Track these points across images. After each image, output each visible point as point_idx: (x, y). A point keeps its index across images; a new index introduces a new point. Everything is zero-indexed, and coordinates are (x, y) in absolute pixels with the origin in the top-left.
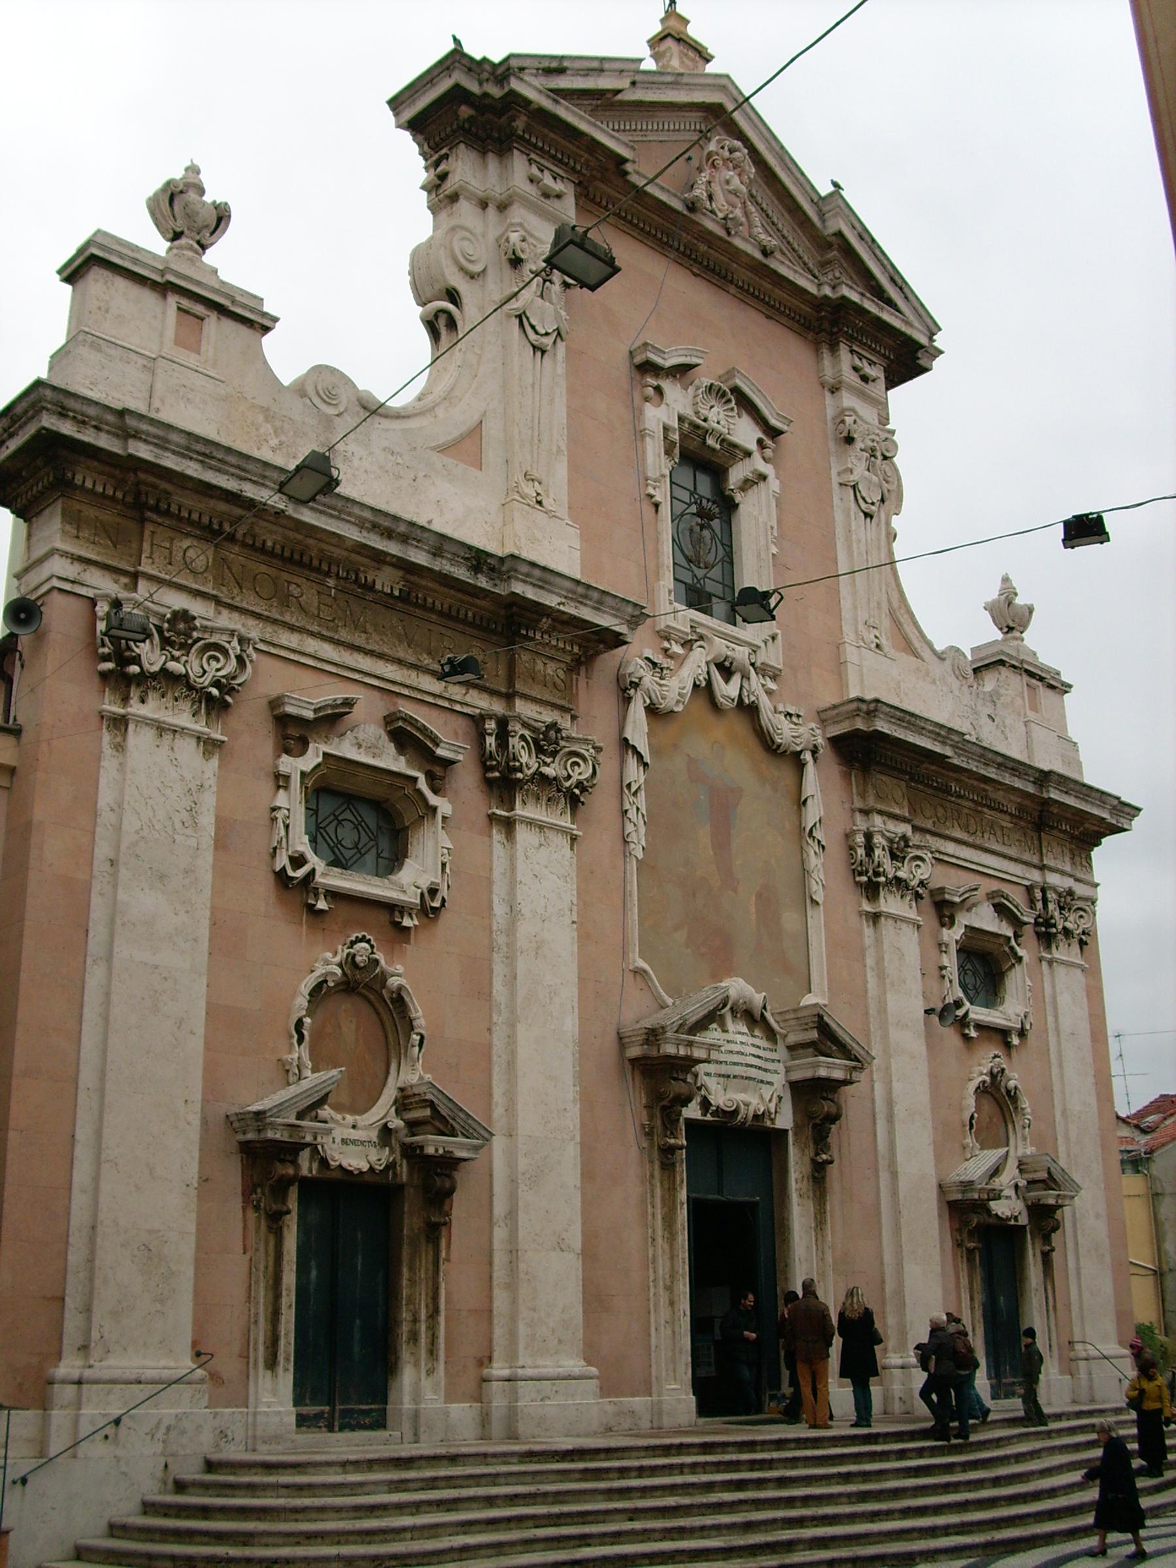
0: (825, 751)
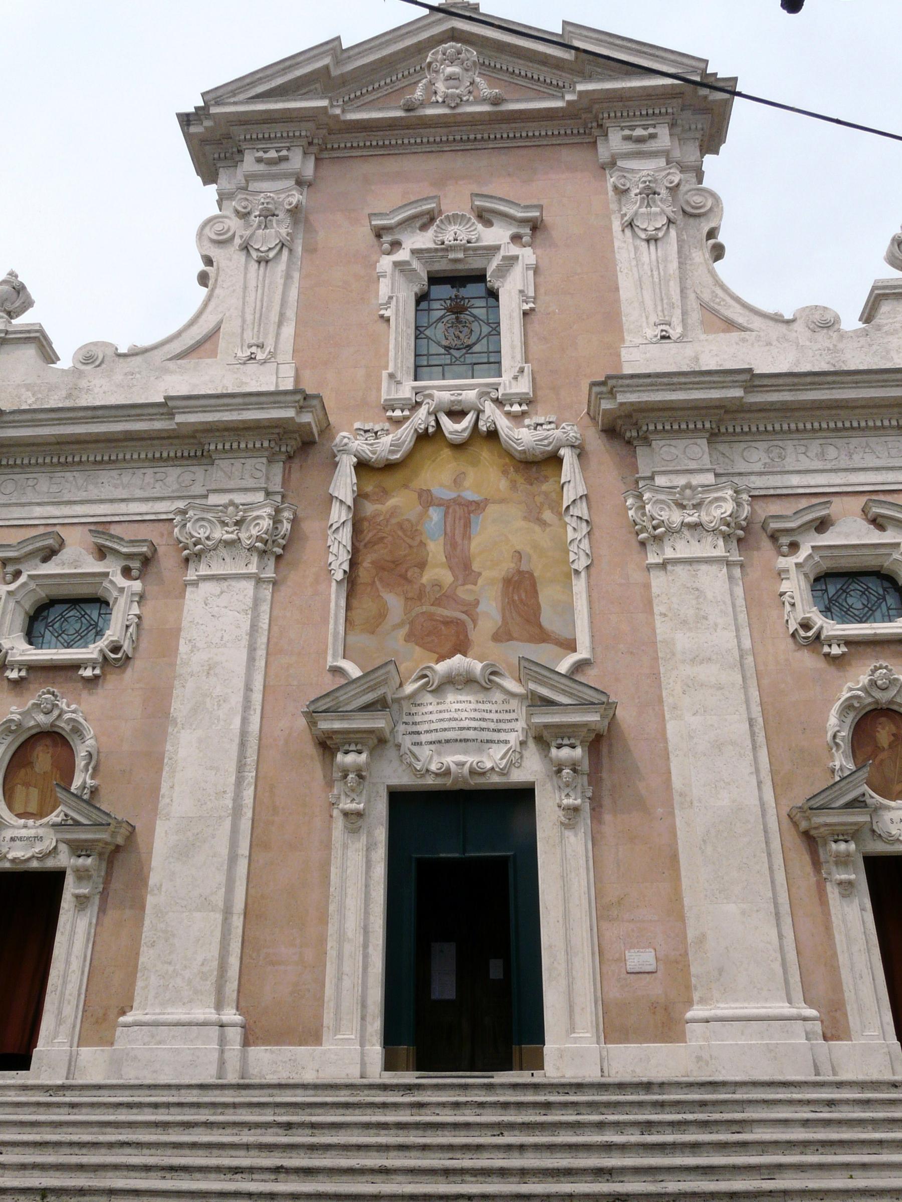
0: (596, 442)
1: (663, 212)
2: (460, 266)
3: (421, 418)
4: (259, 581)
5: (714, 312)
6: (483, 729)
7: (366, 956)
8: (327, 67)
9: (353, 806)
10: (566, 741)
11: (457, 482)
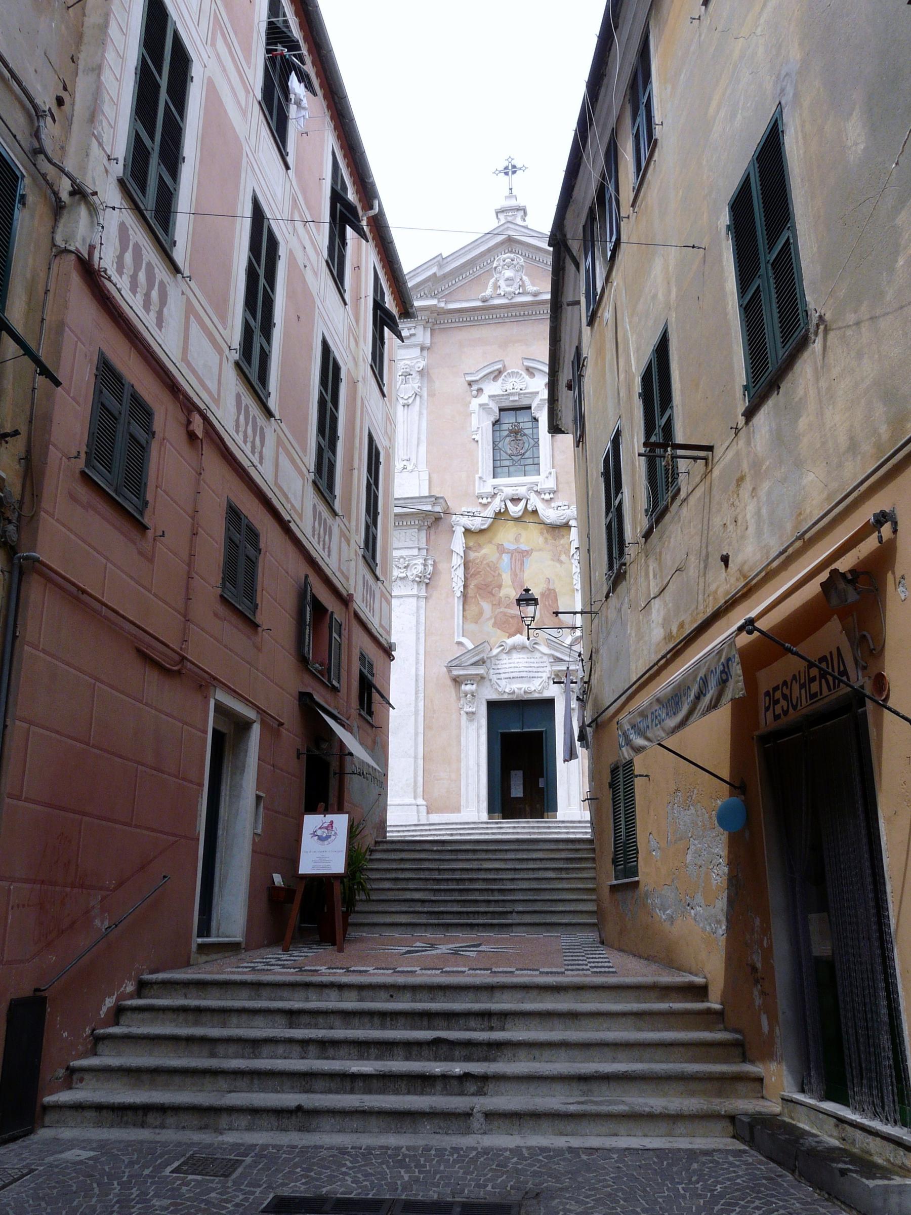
2: (517, 404)
3: (497, 505)
4: (418, 597)
7: (478, 776)
9: (470, 710)
11: (517, 540)
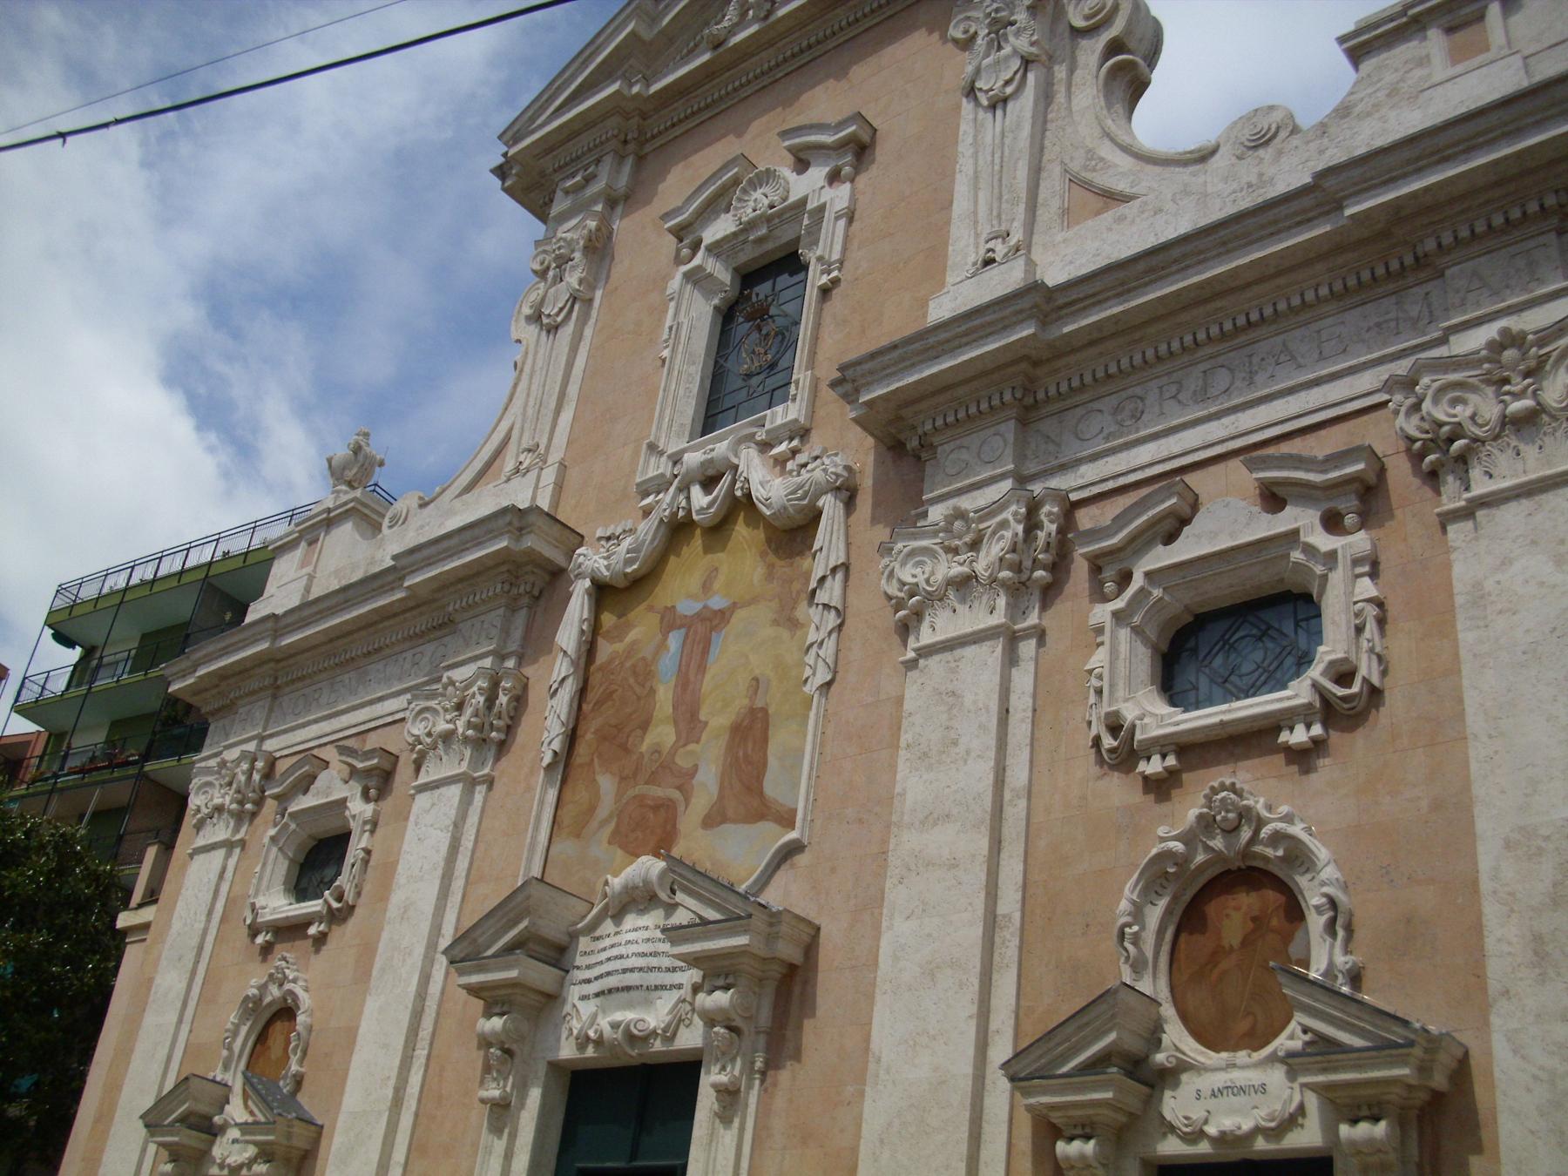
1: (1015, 51)
2: (770, 246)
5: (1087, 186)
6: (651, 969)
8: (633, 34)
10: (721, 982)
